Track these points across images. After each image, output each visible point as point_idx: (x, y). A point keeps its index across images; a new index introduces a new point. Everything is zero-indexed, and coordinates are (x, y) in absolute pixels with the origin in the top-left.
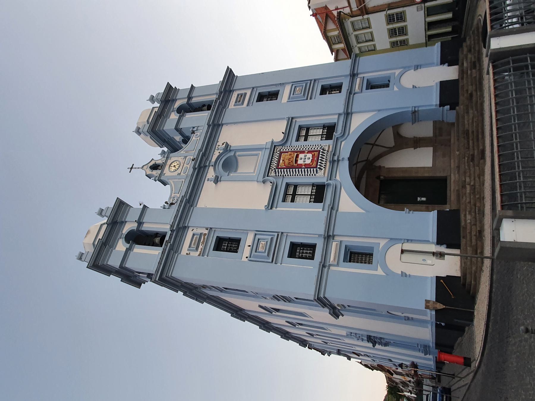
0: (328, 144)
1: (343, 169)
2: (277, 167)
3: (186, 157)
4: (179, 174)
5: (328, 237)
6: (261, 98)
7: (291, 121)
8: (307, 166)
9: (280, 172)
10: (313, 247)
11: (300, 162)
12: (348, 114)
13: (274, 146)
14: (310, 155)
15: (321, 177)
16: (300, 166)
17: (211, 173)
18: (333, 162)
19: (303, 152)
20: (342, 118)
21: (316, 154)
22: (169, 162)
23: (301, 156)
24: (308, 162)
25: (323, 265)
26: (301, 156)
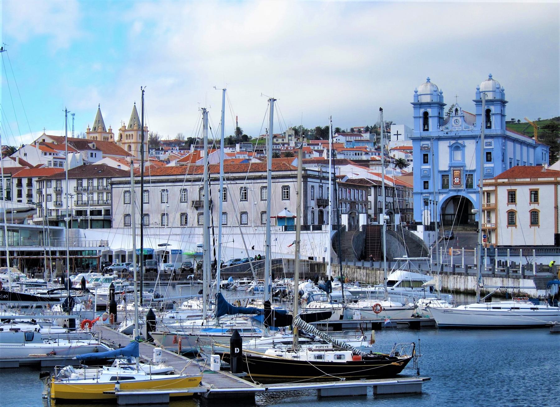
0: (463, 187)
1: (454, 194)
2: (454, 170)
3: (461, 126)
4: (453, 126)
5: (430, 193)
6: (489, 154)
7: (474, 171)
8: (454, 181)
9: (452, 172)
10: (428, 188)
11: (455, 178)
12: (475, 192)
13: (464, 166)
14: (458, 182)
15: (451, 187)
16: (454, 179)
17: (453, 142)
18: (455, 190)
19: (460, 178)
20: (474, 191)
21: (459, 184)
22: (459, 118)
23: (458, 178)
24: (456, 182)
25: (422, 193)
26: (458, 178)
